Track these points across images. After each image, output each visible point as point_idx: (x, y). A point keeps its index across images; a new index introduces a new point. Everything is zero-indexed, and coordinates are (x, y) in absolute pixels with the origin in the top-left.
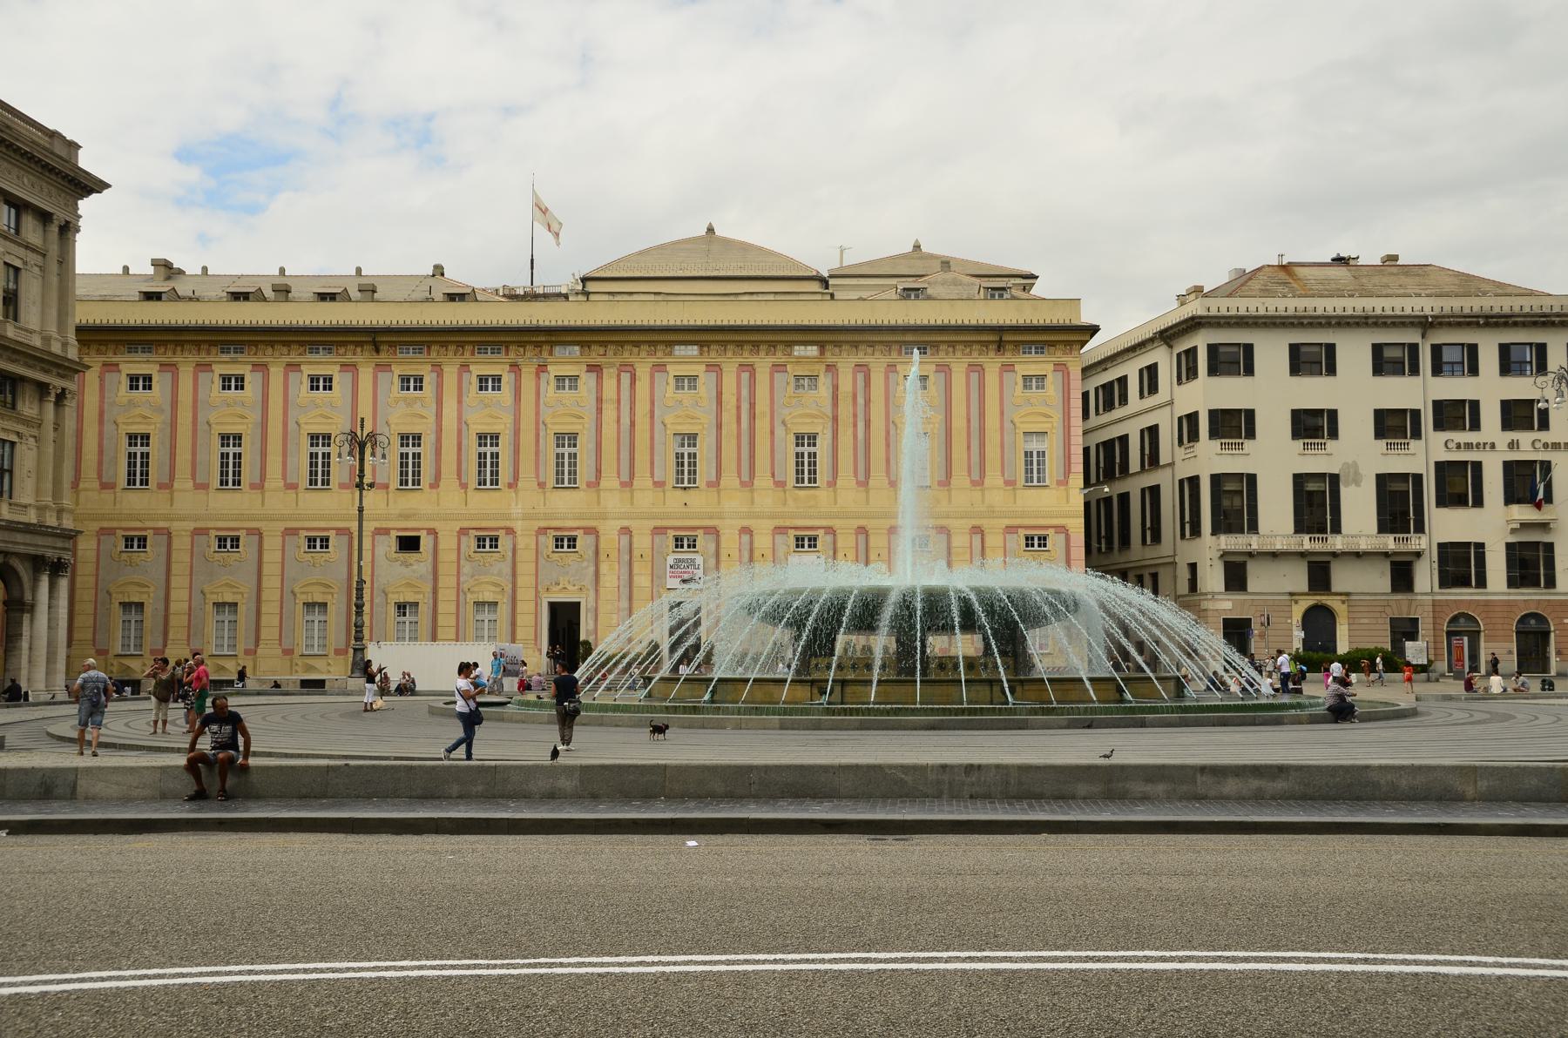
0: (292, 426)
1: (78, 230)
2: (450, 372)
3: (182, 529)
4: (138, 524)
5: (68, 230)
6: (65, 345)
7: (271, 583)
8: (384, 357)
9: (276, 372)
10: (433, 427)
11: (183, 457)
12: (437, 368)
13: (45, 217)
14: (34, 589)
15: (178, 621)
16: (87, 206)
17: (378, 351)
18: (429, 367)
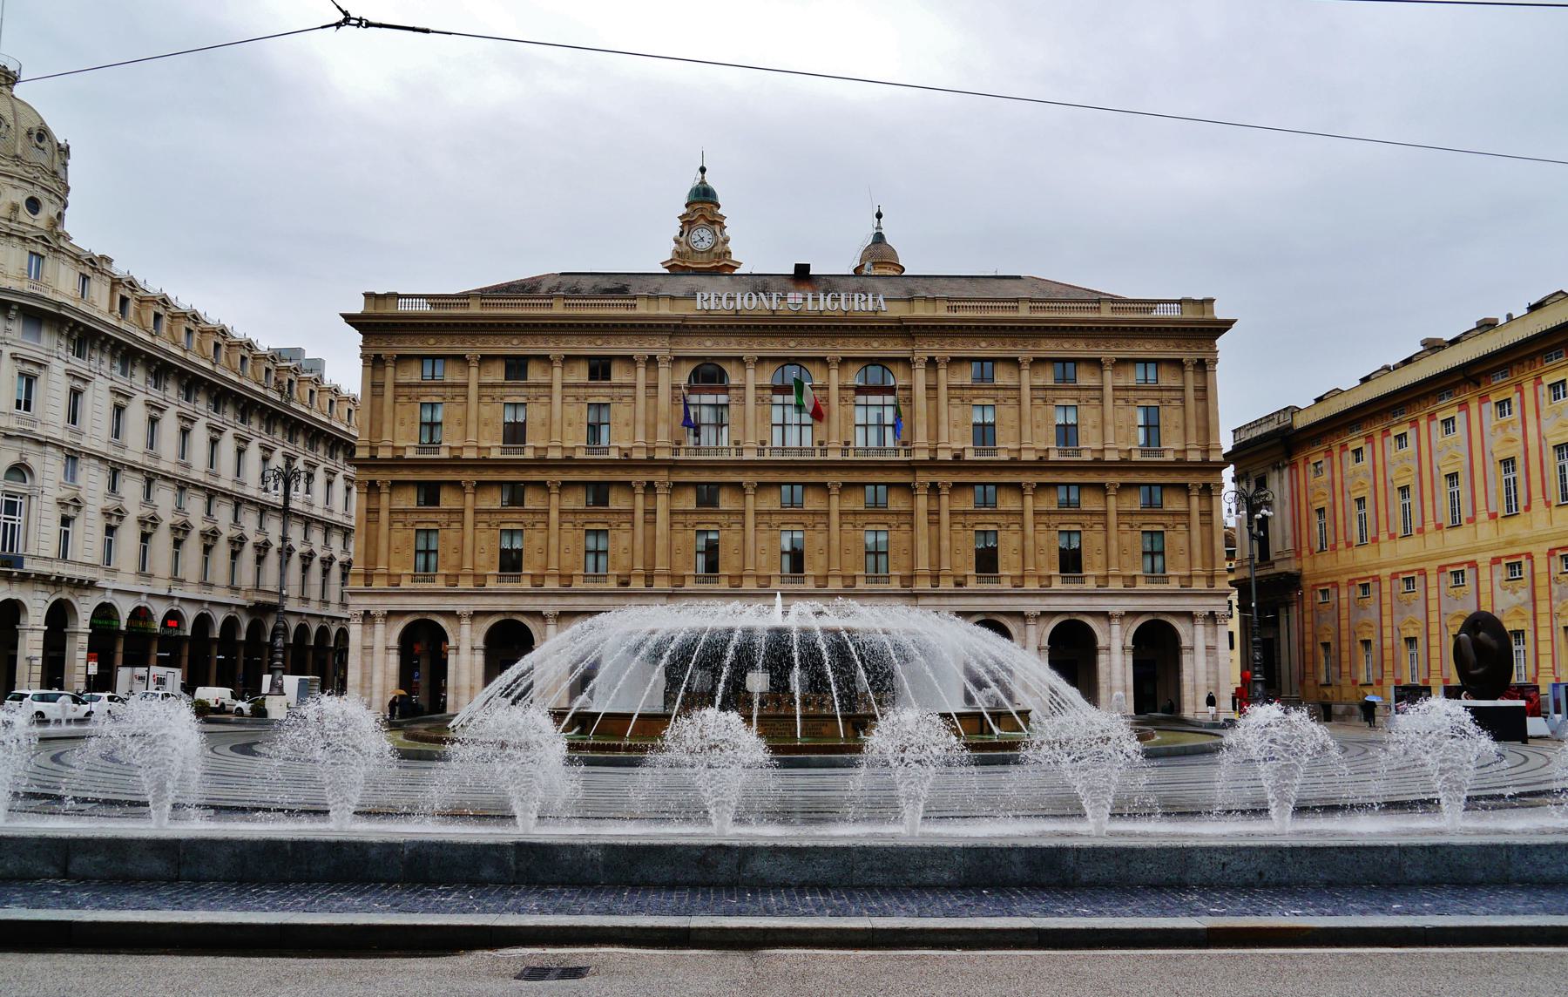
0: (1435, 470)
1: (1215, 362)
2: (1528, 386)
3: (1385, 573)
4: (1364, 574)
5: (1204, 367)
6: (1207, 451)
7: (1434, 618)
8: (1483, 389)
9: (1423, 422)
10: (1522, 448)
11: (1382, 513)
12: (1519, 387)
13: (1178, 364)
14: (1193, 638)
15: (1388, 654)
16: (1221, 342)
17: (1478, 385)
18: (1513, 389)
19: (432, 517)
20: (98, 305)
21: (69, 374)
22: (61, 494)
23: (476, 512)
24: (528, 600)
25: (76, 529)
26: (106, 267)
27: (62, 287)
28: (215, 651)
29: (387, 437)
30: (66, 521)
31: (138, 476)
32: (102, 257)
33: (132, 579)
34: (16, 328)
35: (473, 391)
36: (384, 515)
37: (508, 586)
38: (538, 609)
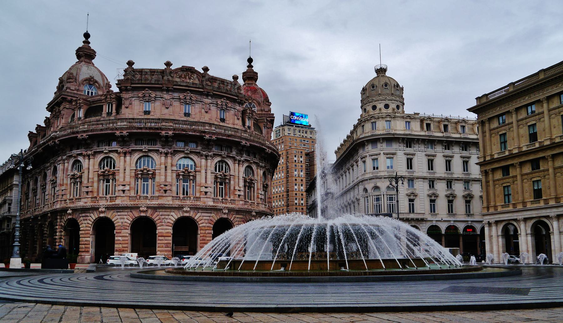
19: (507, 180)
20: (416, 129)
21: (405, 154)
22: (407, 192)
23: (522, 175)
24: (544, 211)
25: (417, 203)
26: (416, 116)
27: (398, 128)
28: (512, 239)
29: (489, 152)
30: (411, 200)
31: (444, 181)
32: (415, 114)
33: (446, 216)
34: (384, 145)
35: (515, 124)
36: (491, 183)
37: (535, 206)
38: (548, 214)
